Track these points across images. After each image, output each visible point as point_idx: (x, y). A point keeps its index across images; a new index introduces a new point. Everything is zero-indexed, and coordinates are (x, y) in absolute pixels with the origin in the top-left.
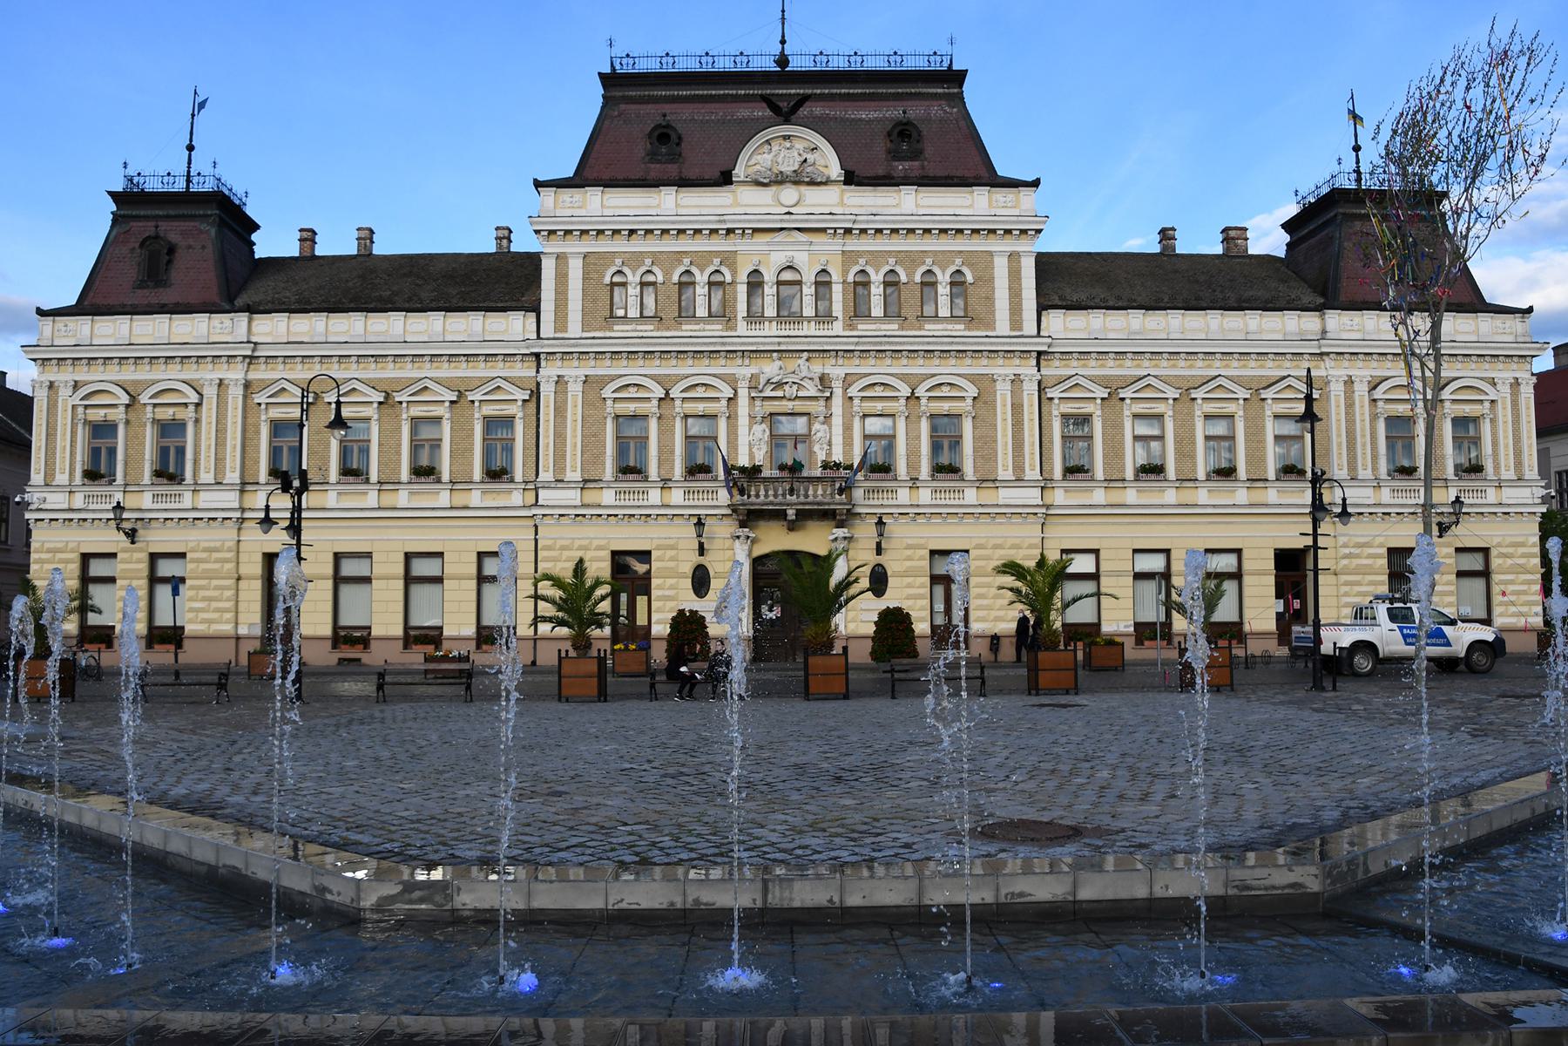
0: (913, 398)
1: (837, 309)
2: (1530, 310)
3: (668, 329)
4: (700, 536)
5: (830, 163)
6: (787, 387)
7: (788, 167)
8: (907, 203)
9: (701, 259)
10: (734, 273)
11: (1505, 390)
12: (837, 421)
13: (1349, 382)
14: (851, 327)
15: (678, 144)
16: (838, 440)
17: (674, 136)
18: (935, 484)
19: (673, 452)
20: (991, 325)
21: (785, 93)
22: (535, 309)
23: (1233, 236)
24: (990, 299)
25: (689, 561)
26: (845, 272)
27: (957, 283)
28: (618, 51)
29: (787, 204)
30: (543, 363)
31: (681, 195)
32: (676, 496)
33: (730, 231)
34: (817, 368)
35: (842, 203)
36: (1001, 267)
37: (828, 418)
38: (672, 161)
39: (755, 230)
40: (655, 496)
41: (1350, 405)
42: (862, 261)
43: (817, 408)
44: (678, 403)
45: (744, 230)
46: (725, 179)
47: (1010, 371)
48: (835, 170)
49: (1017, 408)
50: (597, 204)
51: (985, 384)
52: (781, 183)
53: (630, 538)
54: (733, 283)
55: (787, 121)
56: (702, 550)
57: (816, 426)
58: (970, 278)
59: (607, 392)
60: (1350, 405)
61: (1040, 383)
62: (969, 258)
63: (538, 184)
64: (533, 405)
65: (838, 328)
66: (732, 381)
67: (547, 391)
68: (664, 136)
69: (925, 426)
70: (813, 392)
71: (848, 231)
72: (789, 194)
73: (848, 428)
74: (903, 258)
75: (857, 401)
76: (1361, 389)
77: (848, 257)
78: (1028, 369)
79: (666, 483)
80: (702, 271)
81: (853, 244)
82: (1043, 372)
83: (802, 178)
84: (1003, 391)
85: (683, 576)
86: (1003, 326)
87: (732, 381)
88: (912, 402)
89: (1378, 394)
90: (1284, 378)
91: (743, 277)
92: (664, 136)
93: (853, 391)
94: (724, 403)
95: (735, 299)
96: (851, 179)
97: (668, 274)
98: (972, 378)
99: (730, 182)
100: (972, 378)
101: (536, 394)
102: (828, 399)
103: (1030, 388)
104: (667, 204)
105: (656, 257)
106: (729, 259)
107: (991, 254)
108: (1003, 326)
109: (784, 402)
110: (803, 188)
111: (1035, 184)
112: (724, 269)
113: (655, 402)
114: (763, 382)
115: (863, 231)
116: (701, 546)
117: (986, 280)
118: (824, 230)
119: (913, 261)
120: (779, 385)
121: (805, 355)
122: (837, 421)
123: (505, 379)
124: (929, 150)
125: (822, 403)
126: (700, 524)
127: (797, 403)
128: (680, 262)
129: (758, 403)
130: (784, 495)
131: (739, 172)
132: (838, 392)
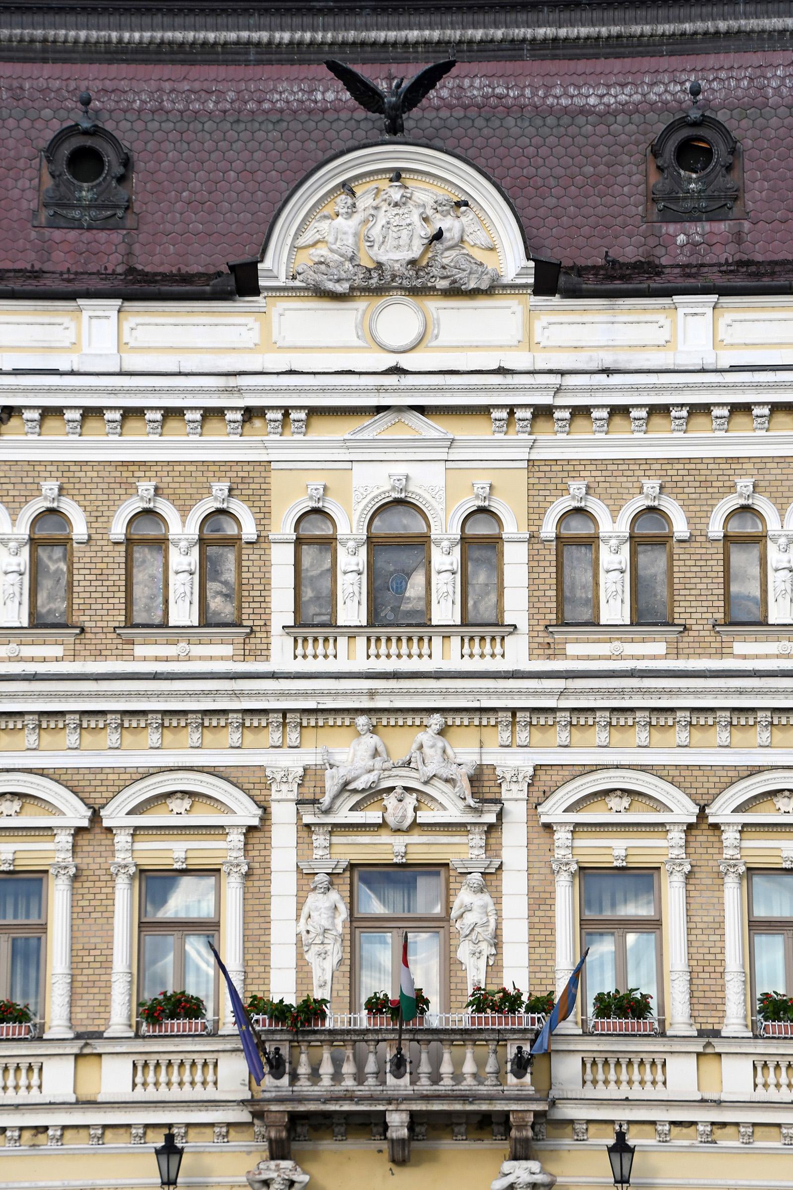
3: (99, 655)
5: (500, 242)
6: (390, 801)
7: (396, 254)
8: (691, 335)
10: (263, 517)
12: (515, 884)
14: (550, 650)
15: (122, 179)
16: (516, 933)
17: (110, 157)
18: (761, 1047)
19: (107, 964)
26: (535, 514)
31: (131, 321)
32: (114, 1078)
33: (251, 413)
34: (466, 752)
35: (529, 343)
37: (491, 878)
38: (106, 225)
39: (314, 412)
40: (58, 1079)
42: (577, 487)
43: (465, 851)
44: (122, 840)
46: (241, 282)
48: (512, 261)
52: (379, 291)
57: (464, 897)
65: (516, 653)
68: (85, 156)
70: (454, 813)
71: (542, 412)
72: (398, 319)
73: (540, 902)
74: (679, 475)
75: (562, 836)
77: (543, 476)
79: (87, 1043)
80: (184, 512)
88: (702, 837)
91: (284, 527)
92: (85, 156)
93: (553, 810)
94: (236, 838)
95: (266, 584)
96: (549, 280)
97: (98, 518)
99: (253, 289)
102: (491, 829)
104: (95, 337)
105: (69, 475)
106: (250, 481)
109: (385, 838)
110: (433, 305)
112: (238, 507)
113: (64, 839)
114: (331, 786)
115: (581, 412)
118: (484, 411)
119: (706, 484)
120: (374, 795)
121: (436, 721)
122: (515, 884)
124: (756, 192)
125: (477, 839)
127: (415, 838)
128: (130, 489)
129: (320, 839)
130: (380, 1075)
131: (275, 266)
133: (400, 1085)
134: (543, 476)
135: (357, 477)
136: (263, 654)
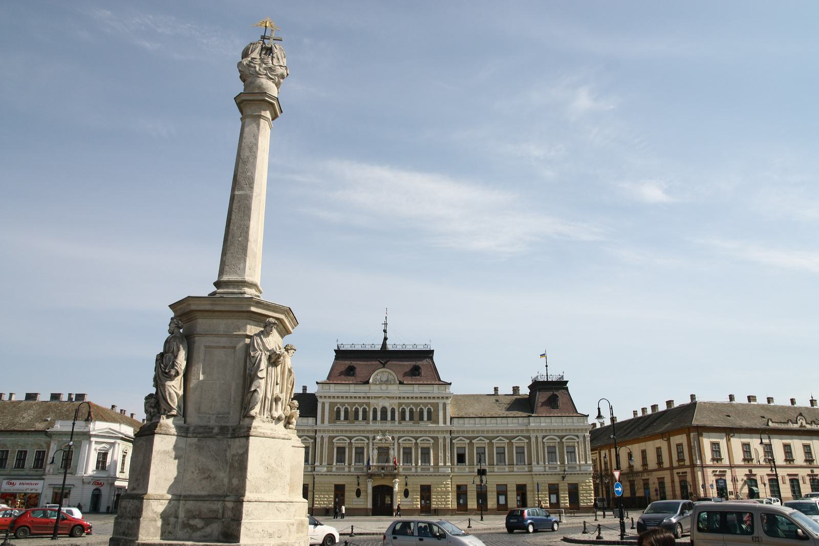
0: (416, 444)
1: (397, 418)
2: (588, 415)
4: (358, 481)
9: (361, 404)
10: (369, 408)
11: (581, 439)
13: (537, 437)
20: (438, 423)
21: (384, 356)
22: (315, 416)
23: (516, 389)
24: (438, 416)
25: (355, 488)
27: (429, 412)
28: (339, 343)
29: (384, 389)
30: (317, 432)
36: (441, 406)
37: (393, 449)
39: (375, 397)
41: (537, 443)
42: (403, 405)
45: (372, 397)
46: (367, 382)
47: (443, 435)
49: (445, 446)
50: (334, 390)
51: (436, 439)
53: (340, 481)
54: (369, 411)
55: (384, 367)
56: (358, 484)
58: (432, 410)
59: (334, 440)
60: (537, 443)
61: (451, 439)
62: (432, 404)
63: (317, 383)
64: (314, 443)
66: (368, 438)
67: (318, 440)
69: (420, 450)
72: (384, 387)
74: (414, 404)
76: (540, 439)
78: (448, 436)
81: (402, 401)
82: (452, 435)
83: (387, 382)
84: (441, 441)
85: (353, 491)
86: (441, 424)
87: (368, 438)
89: (544, 440)
90: (518, 436)
91: (372, 409)
93: (400, 441)
98: (432, 438)
100: (432, 438)
101: (315, 439)
103: (448, 441)
105: (348, 403)
107: (438, 403)
108: (441, 424)
111: (450, 384)
116: (359, 483)
117: (437, 411)
123: (307, 436)
126: (358, 477)
132: (396, 441)
133: (383, 471)
134: (400, 404)
135: (379, 404)
136: (369, 423)
